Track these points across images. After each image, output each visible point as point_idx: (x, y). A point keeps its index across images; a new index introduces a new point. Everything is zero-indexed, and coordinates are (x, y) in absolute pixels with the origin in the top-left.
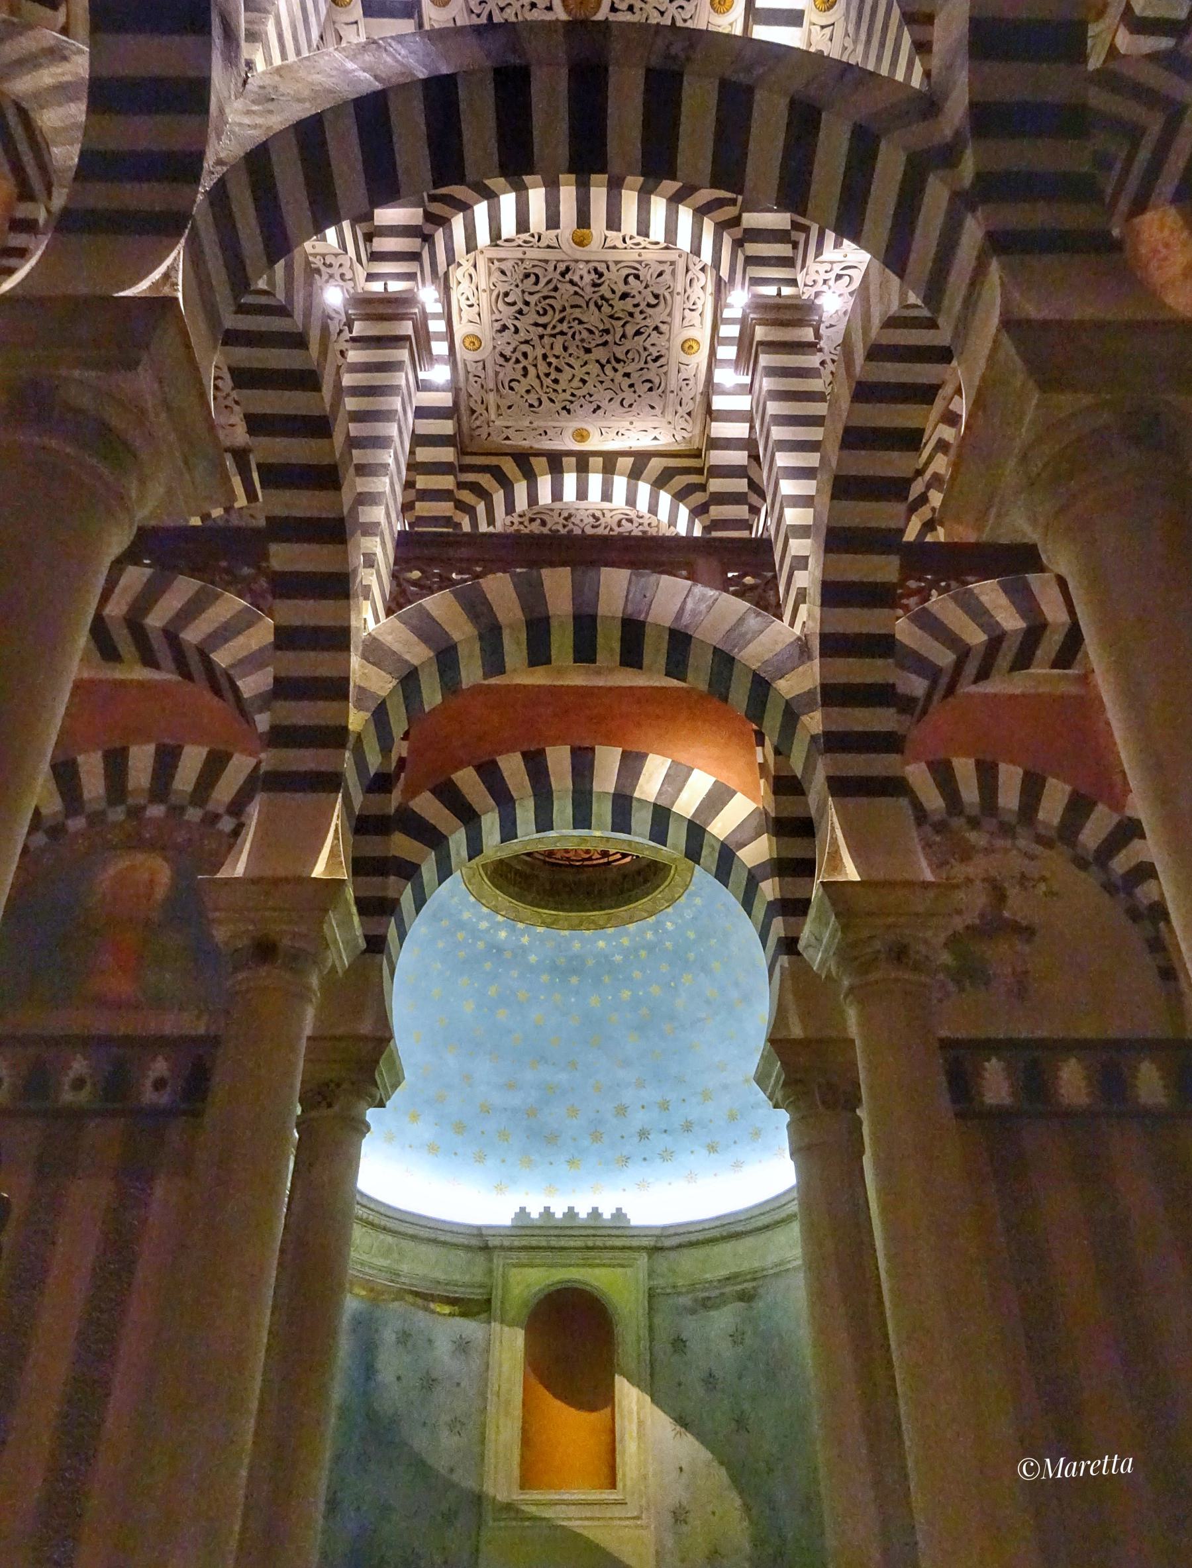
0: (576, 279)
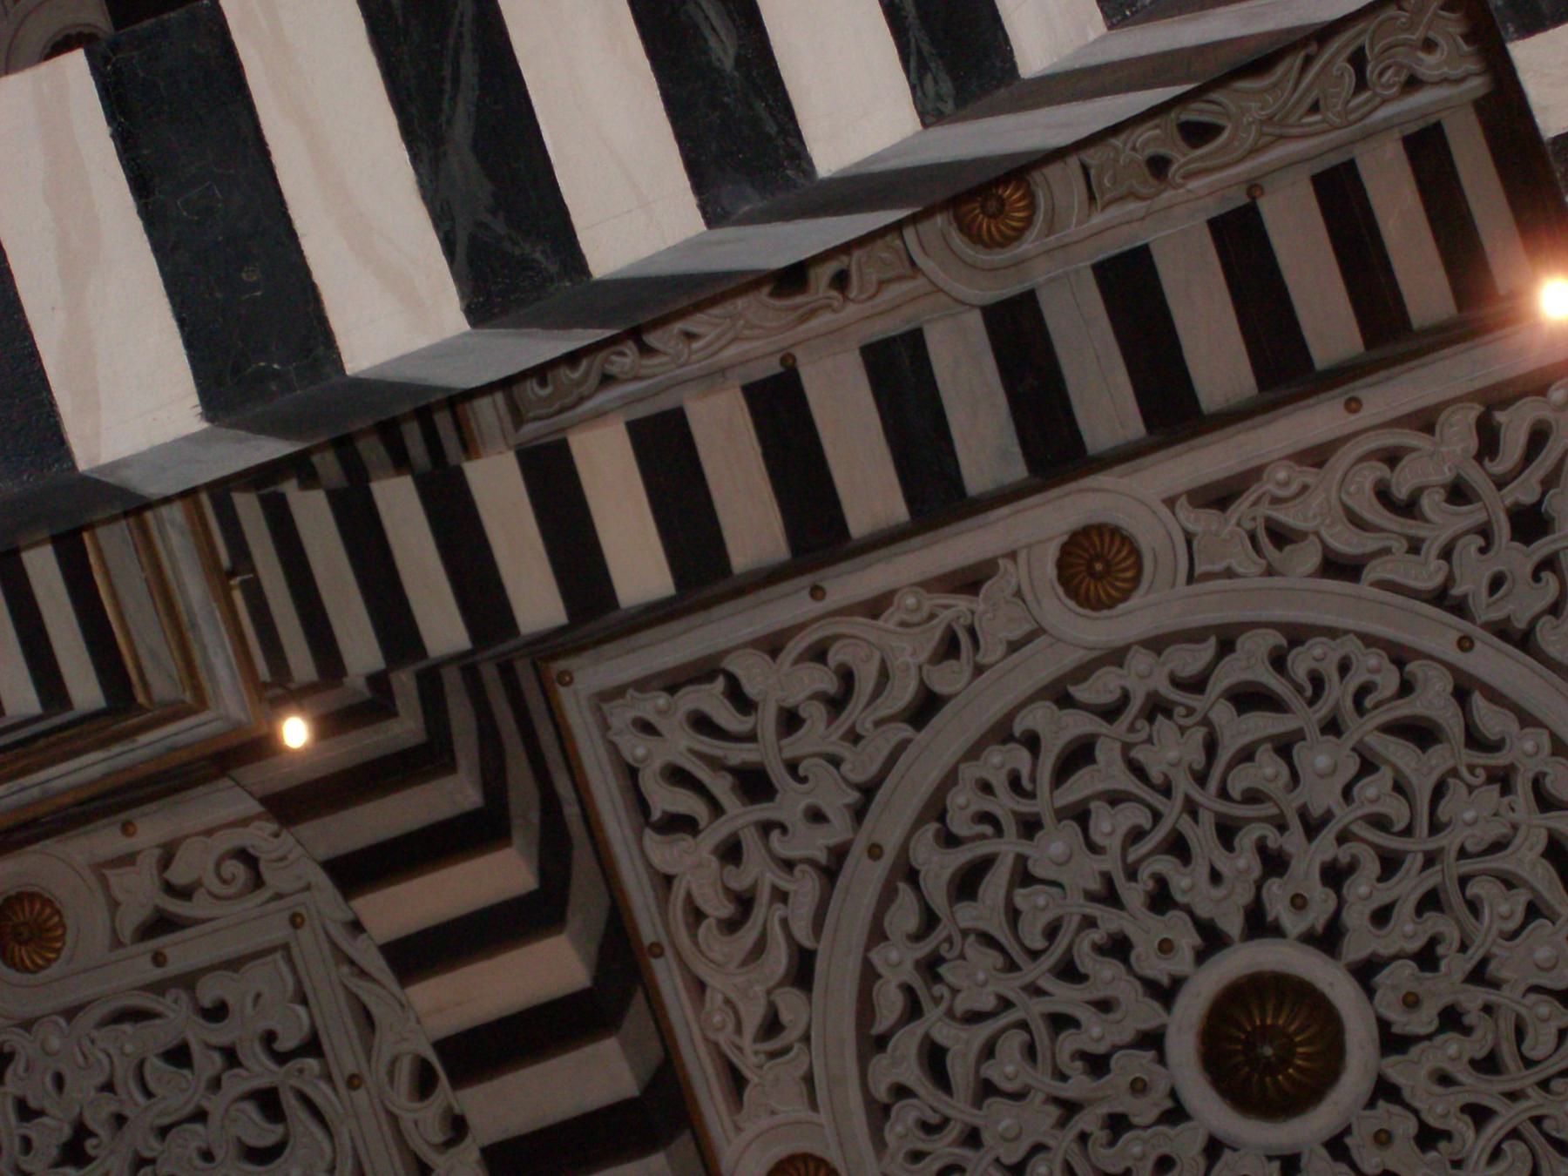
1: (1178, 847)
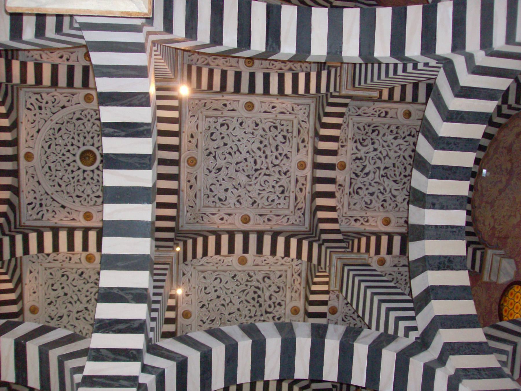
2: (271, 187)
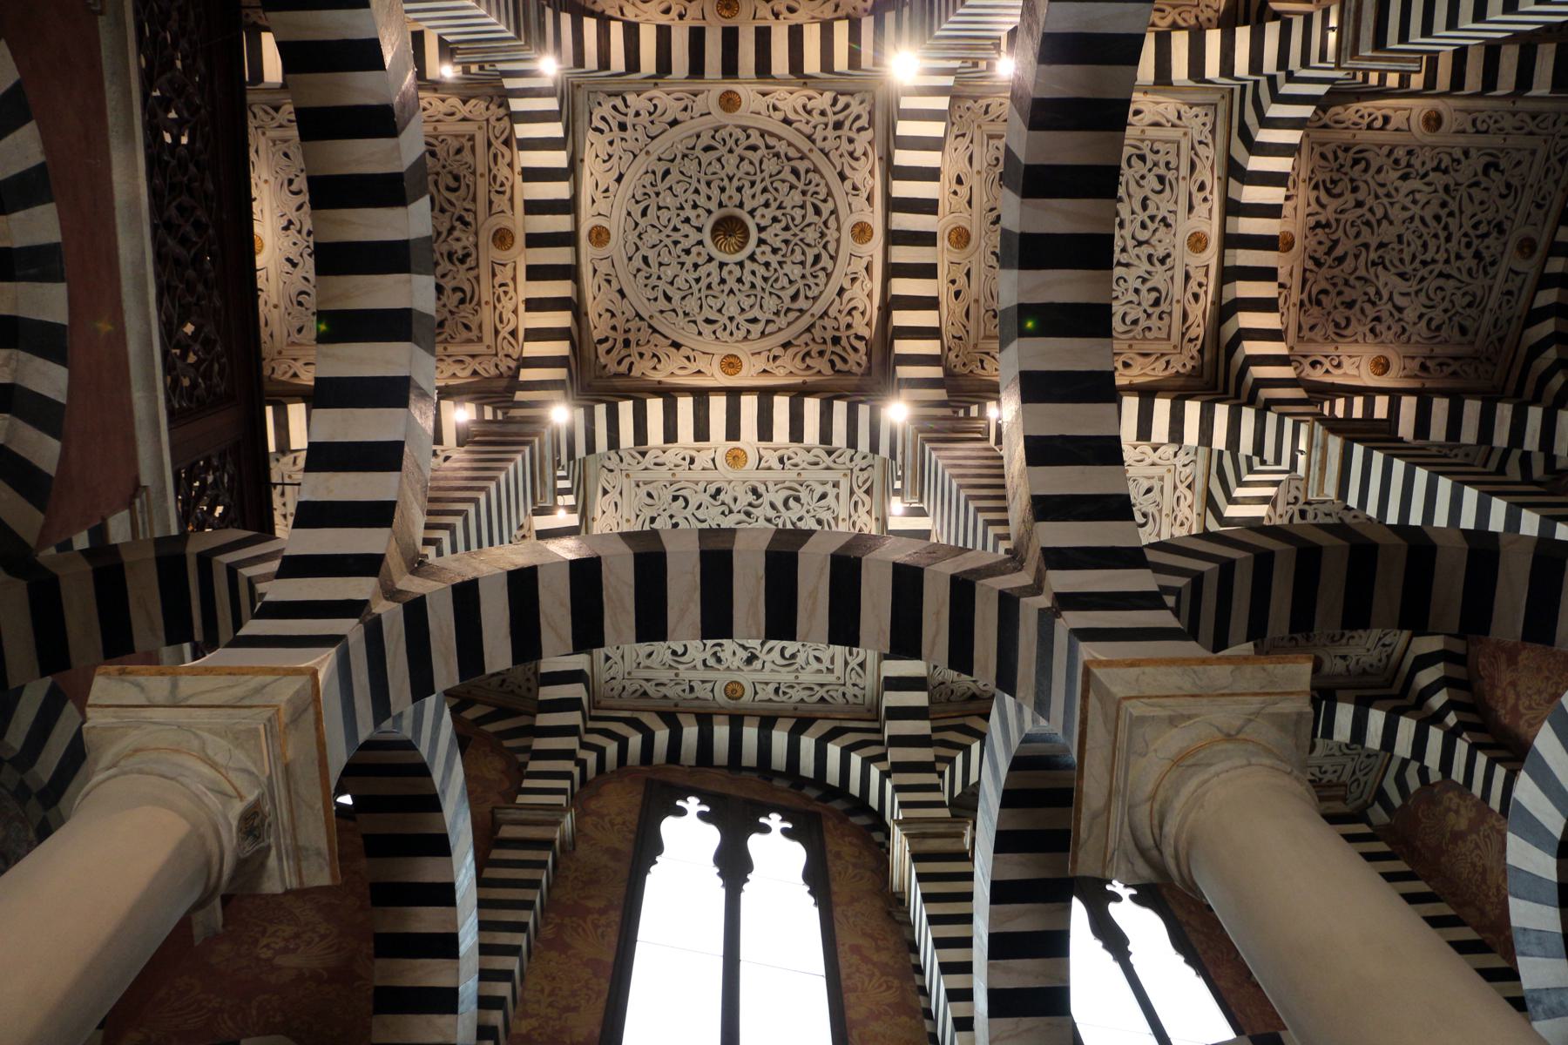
0: (456, 234)
1: (787, 228)
2: (1131, 291)
